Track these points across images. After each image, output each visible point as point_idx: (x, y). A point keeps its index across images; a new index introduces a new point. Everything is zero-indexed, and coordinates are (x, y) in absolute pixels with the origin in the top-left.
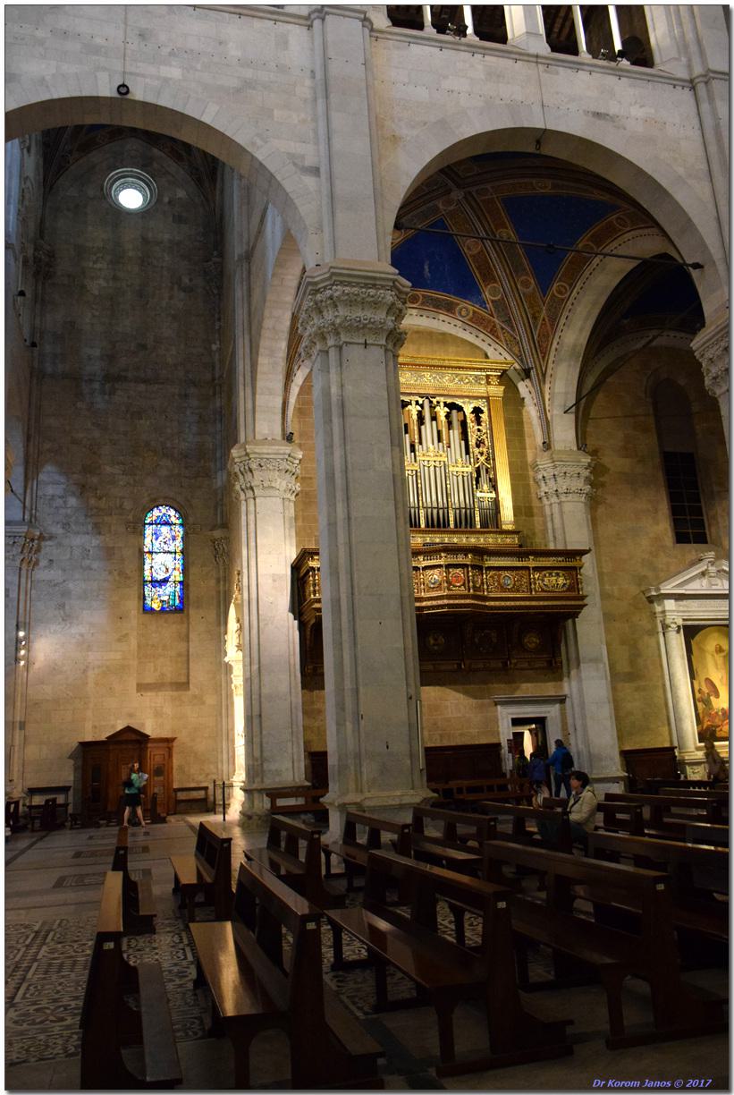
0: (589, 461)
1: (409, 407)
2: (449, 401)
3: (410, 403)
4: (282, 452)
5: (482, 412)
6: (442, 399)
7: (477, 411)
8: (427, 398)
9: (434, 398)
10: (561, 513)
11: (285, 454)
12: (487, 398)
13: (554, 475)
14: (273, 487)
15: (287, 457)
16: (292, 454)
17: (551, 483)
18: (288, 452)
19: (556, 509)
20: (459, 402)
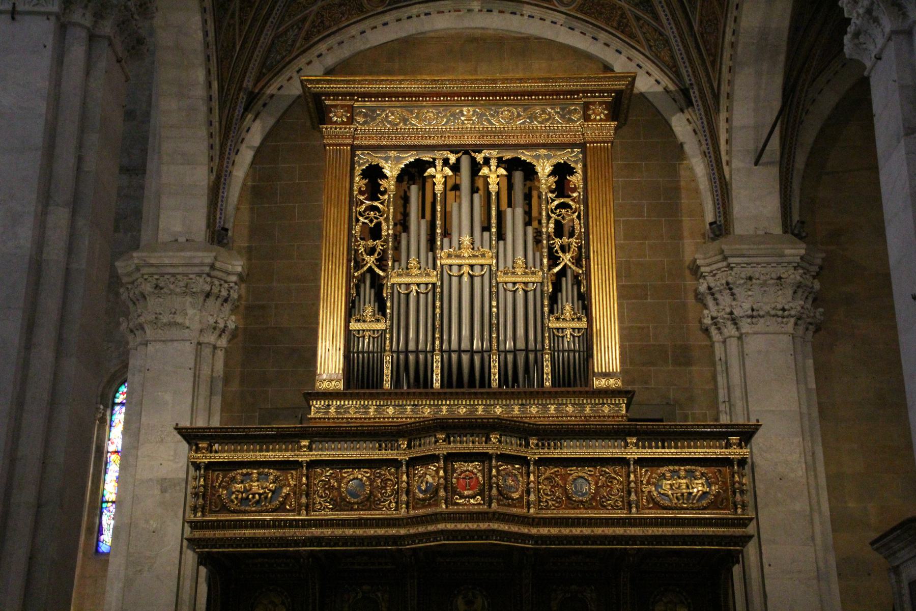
0: (803, 252)
1: (431, 171)
2: (508, 155)
3: (432, 164)
4: (197, 261)
5: (571, 171)
6: (494, 153)
7: (562, 171)
8: (466, 152)
9: (480, 152)
10: (742, 355)
11: (202, 265)
12: (583, 146)
13: (728, 284)
14: (176, 324)
15: (207, 269)
16: (218, 265)
17: (725, 299)
18: (208, 260)
19: (733, 344)
20: (526, 156)
